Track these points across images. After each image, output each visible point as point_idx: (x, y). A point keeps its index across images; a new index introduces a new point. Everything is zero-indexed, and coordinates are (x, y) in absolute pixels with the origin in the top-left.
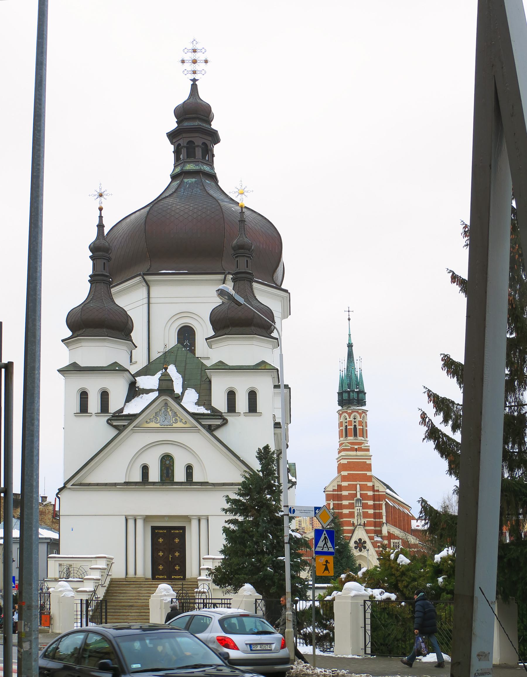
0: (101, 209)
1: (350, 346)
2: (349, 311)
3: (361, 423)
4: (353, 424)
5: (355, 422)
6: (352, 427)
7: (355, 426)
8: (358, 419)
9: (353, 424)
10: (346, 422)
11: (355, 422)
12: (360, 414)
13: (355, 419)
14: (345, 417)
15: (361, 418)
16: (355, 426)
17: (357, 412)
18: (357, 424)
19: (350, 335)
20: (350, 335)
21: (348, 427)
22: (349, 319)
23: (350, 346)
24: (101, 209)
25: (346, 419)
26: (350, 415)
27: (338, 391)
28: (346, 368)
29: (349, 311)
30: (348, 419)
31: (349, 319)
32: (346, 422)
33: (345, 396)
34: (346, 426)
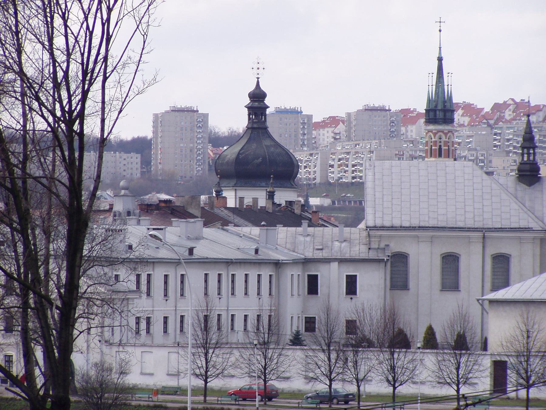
0: (258, 78)
1: (440, 59)
2: (440, 22)
3: (446, 143)
4: (438, 144)
5: (440, 142)
6: (437, 148)
7: (440, 146)
8: (444, 139)
9: (438, 144)
10: (431, 142)
11: (440, 142)
12: (446, 134)
13: (440, 138)
14: (431, 136)
15: (446, 138)
16: (440, 146)
17: (443, 132)
18: (442, 144)
19: (440, 48)
20: (440, 48)
21: (433, 148)
22: (440, 31)
23: (440, 59)
24: (258, 78)
25: (432, 139)
26: (435, 134)
27: (425, 108)
28: (434, 83)
29: (440, 22)
30: (433, 140)
31: (440, 31)
32: (431, 142)
33: (432, 115)
34: (431, 146)
